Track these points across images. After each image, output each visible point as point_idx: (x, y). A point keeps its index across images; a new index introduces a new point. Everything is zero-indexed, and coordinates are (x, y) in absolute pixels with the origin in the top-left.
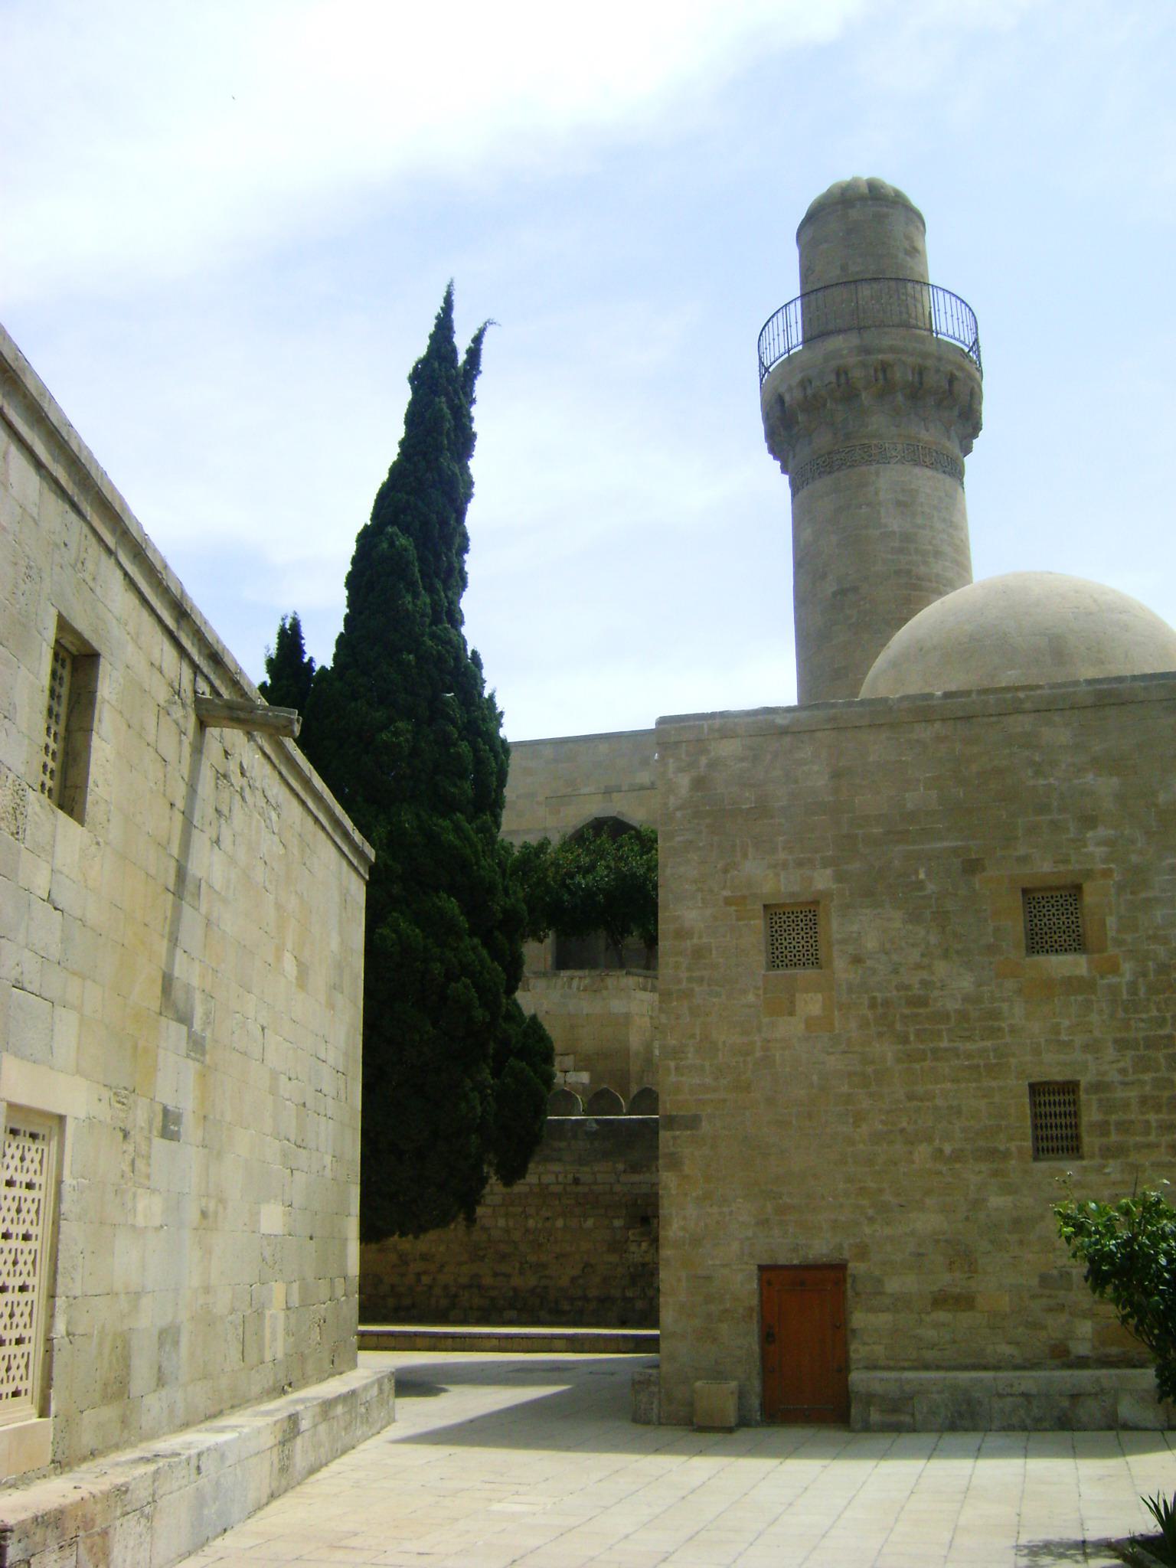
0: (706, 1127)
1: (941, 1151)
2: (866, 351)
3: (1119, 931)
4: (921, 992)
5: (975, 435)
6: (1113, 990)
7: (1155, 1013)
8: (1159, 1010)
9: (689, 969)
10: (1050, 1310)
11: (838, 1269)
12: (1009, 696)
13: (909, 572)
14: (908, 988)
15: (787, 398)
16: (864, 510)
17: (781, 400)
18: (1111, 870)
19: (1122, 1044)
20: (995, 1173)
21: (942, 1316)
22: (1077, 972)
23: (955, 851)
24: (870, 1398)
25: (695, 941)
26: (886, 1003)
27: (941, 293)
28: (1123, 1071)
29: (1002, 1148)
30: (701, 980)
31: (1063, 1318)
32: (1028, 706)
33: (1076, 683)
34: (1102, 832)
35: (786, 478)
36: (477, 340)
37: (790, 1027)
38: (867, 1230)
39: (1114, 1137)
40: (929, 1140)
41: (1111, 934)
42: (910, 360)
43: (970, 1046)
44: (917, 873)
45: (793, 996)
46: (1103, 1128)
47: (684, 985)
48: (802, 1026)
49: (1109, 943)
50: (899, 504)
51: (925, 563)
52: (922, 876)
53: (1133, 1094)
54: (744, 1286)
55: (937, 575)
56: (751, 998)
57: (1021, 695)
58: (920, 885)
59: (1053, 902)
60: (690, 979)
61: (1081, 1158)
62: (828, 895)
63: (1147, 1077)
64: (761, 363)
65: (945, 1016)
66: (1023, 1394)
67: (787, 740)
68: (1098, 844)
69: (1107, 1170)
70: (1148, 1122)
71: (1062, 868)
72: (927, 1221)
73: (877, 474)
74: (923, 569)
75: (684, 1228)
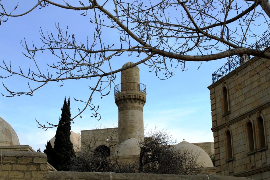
2: (127, 94)
16: (127, 116)
36: (69, 100)
51: (135, 124)
57: (126, 157)
74: (134, 125)
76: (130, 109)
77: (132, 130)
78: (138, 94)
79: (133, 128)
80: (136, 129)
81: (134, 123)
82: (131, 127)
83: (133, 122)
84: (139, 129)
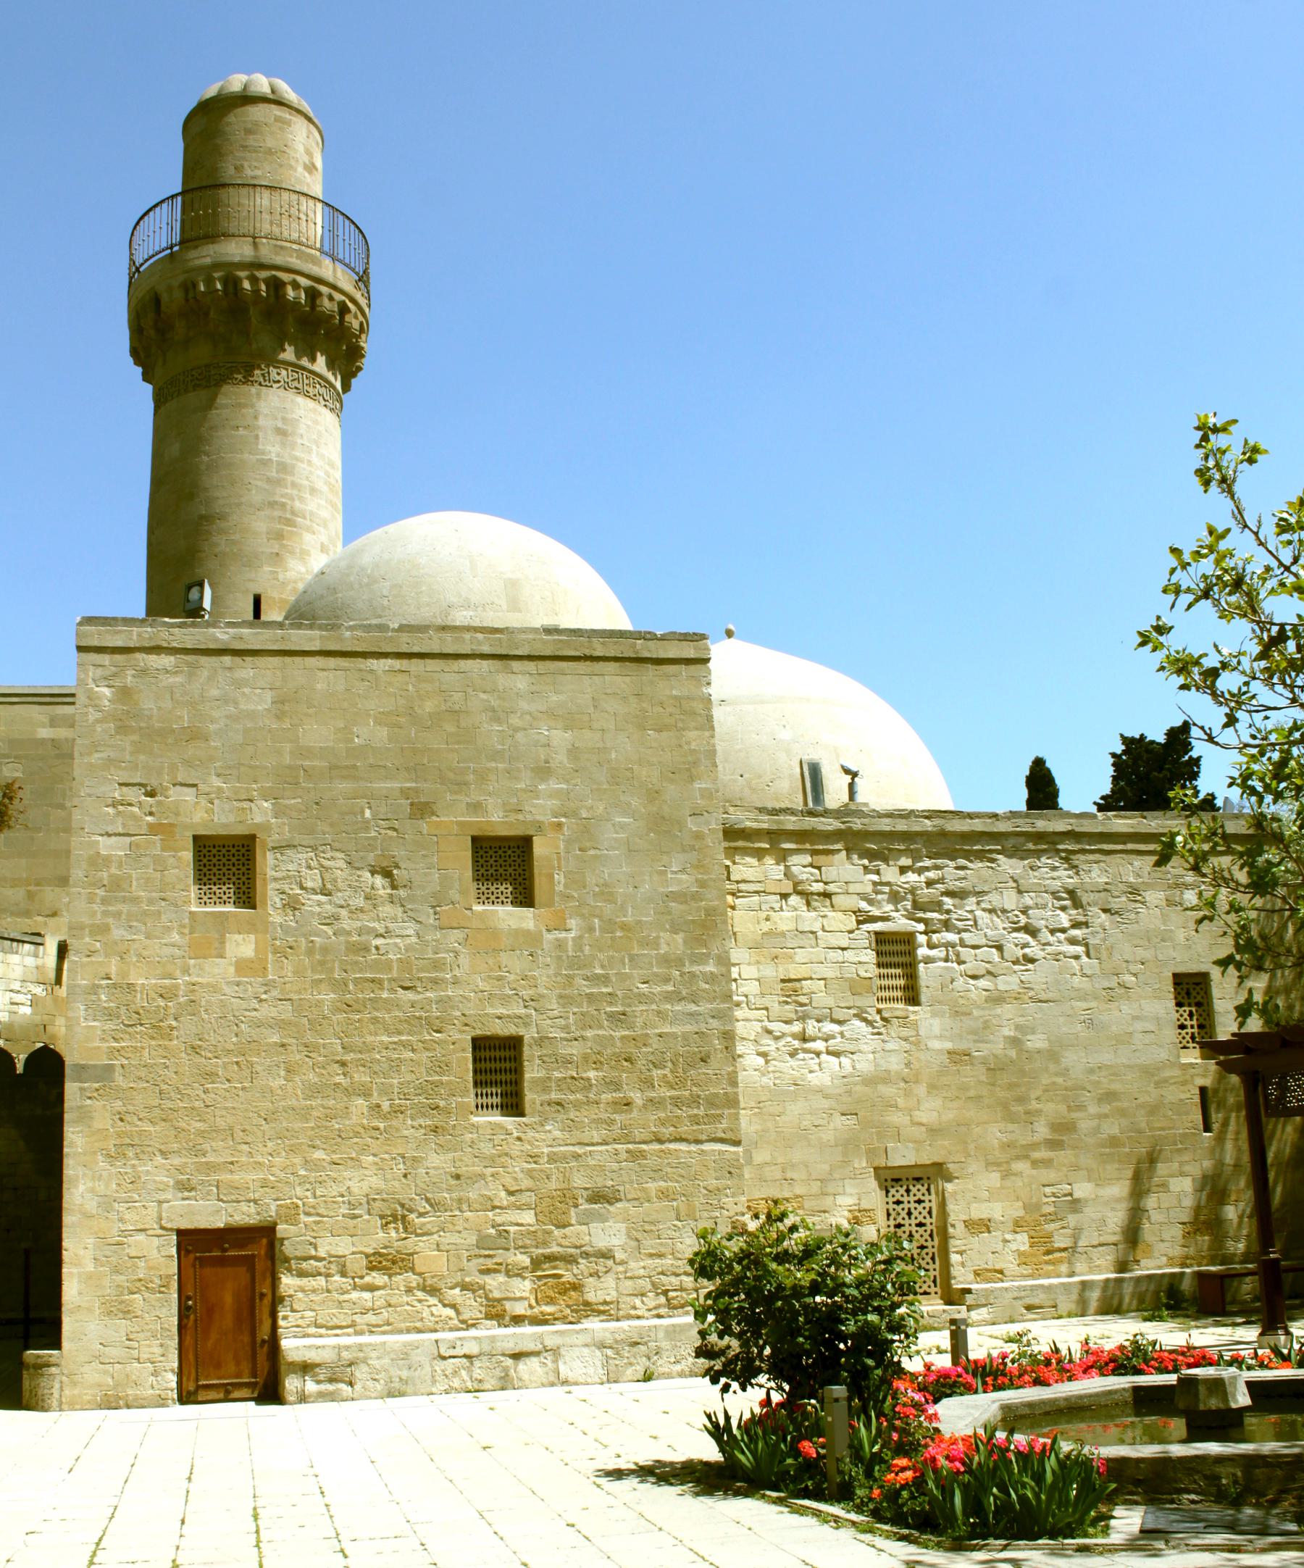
0: (119, 1080)
1: (378, 1106)
3: (566, 886)
4: (364, 938)
5: (354, 375)
6: (560, 945)
7: (599, 971)
8: (603, 967)
9: (104, 901)
10: (487, 1271)
11: (266, 1233)
12: (467, 636)
13: (283, 505)
14: (349, 933)
15: (165, 298)
16: (241, 432)
17: (157, 301)
18: (560, 825)
19: (565, 1000)
20: (435, 1130)
21: (377, 1278)
22: (524, 925)
23: (405, 793)
24: (306, 1368)
25: (114, 870)
26: (325, 950)
27: (341, 217)
28: (566, 1028)
29: (442, 1104)
30: (118, 915)
31: (501, 1278)
32: (486, 649)
33: (535, 630)
34: (554, 785)
35: (148, 389)
37: (218, 971)
38: (299, 1191)
39: (554, 1096)
40: (366, 1094)
41: (559, 888)
42: (304, 282)
43: (410, 995)
44: (363, 812)
45: (223, 936)
46: (544, 1085)
47: (98, 919)
48: (232, 969)
49: (557, 899)
50: (281, 432)
51: (301, 498)
52: (368, 814)
53: (575, 1050)
54: (161, 1256)
55: (312, 513)
56: (176, 937)
58: (366, 826)
59: (500, 852)
60: (105, 913)
61: (522, 1115)
62: (266, 827)
63: (589, 1033)
64: (132, 262)
65: (388, 966)
66: (465, 1356)
67: (227, 660)
68: (550, 796)
69: (548, 1128)
70: (589, 1079)
71: (512, 818)
72: (362, 1181)
73: (258, 395)
74: (297, 504)
75: (92, 1190)
76: (267, 382)
77: (280, 536)
78: (334, 287)
79: (289, 522)
80: (307, 537)
81: (294, 485)
82: (277, 513)
83: (289, 478)
84: (324, 539)
